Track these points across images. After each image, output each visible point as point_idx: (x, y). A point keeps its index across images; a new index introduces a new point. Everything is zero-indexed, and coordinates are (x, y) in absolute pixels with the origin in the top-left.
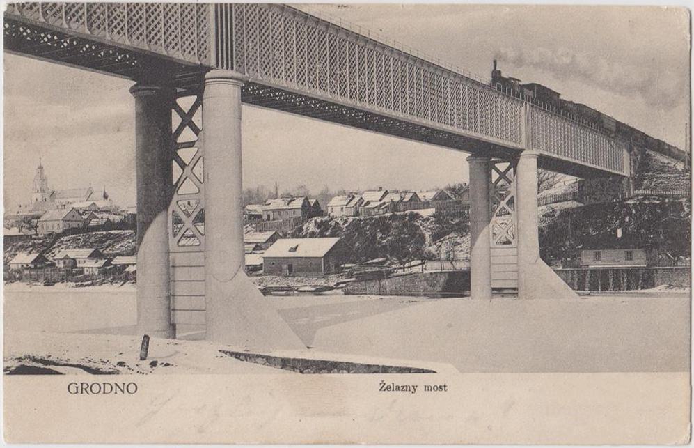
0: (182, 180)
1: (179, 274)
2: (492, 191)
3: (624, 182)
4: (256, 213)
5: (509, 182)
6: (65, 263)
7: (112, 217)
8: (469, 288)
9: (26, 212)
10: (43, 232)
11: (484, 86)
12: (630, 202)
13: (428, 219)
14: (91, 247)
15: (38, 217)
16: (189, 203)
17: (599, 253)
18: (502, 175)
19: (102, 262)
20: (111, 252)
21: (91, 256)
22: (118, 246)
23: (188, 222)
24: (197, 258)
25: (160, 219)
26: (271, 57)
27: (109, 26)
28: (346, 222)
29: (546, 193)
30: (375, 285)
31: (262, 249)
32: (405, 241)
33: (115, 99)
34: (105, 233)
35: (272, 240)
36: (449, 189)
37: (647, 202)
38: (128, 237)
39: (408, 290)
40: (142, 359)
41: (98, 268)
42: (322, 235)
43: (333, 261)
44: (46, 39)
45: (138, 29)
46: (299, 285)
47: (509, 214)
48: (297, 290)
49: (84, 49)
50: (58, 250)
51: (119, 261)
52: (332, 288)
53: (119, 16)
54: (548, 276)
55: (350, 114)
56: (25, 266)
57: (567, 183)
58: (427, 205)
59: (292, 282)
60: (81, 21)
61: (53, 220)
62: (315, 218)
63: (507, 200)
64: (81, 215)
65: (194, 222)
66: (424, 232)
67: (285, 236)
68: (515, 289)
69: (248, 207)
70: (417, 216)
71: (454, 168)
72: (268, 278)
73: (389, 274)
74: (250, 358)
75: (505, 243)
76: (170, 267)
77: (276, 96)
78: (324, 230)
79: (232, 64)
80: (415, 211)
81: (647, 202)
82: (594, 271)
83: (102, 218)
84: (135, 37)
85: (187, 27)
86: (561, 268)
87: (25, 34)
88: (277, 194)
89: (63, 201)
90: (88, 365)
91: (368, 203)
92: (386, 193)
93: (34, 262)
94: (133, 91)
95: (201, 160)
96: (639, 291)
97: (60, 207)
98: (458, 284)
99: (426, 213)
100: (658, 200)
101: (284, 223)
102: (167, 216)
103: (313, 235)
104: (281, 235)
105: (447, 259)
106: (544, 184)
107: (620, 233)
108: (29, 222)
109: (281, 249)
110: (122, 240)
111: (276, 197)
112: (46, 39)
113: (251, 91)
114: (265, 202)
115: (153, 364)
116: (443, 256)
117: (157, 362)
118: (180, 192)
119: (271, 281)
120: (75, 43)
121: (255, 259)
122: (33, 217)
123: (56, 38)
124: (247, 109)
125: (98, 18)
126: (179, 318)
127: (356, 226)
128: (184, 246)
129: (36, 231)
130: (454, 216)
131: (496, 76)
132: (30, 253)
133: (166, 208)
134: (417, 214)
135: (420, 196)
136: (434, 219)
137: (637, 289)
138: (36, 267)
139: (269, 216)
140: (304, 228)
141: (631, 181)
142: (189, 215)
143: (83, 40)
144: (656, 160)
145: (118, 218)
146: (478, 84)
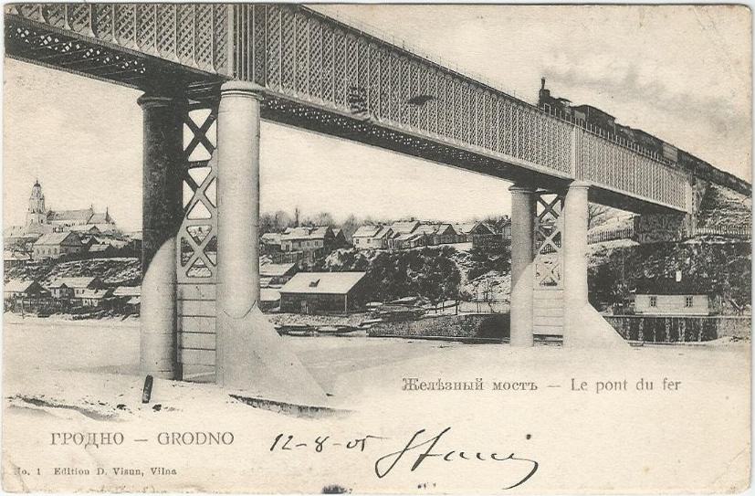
0: (194, 201)
1: (188, 308)
2: (536, 228)
3: (686, 219)
4: (274, 243)
5: (556, 216)
6: (61, 292)
7: (114, 243)
9: (18, 234)
10: (38, 258)
11: (530, 107)
13: (465, 255)
14: (92, 276)
15: (34, 241)
16: (200, 229)
17: (655, 299)
18: (549, 208)
19: (102, 293)
20: (112, 281)
21: (91, 286)
22: (120, 275)
23: (199, 249)
24: (208, 291)
26: (294, 69)
27: (116, 29)
28: (373, 253)
29: (597, 229)
30: (402, 327)
31: (278, 283)
32: (438, 279)
33: (119, 113)
34: (106, 260)
35: (291, 273)
36: (489, 222)
37: (710, 242)
38: (132, 265)
39: (439, 334)
40: (144, 402)
41: (98, 299)
42: (345, 269)
44: (46, 42)
45: (147, 33)
46: (319, 324)
47: (555, 251)
48: (317, 330)
49: (88, 54)
50: (54, 277)
51: (121, 292)
52: (355, 329)
53: (127, 18)
54: (597, 325)
55: (381, 133)
56: (18, 294)
57: (621, 219)
58: (463, 239)
60: (86, 23)
61: (50, 243)
62: (339, 250)
63: (552, 237)
64: (82, 239)
65: (205, 250)
66: (461, 269)
67: (305, 270)
68: (558, 336)
69: (265, 236)
70: (453, 251)
71: (490, 199)
72: (286, 316)
73: (418, 316)
74: (264, 404)
75: (549, 284)
76: (176, 299)
77: (298, 112)
78: (348, 264)
79: (251, 75)
80: (450, 245)
81: (710, 242)
82: (649, 319)
83: (103, 243)
84: (144, 41)
85: (202, 31)
86: (612, 315)
87: (23, 35)
88: (297, 222)
89: (62, 223)
90: (85, 407)
91: (398, 235)
92: (419, 224)
93: (29, 290)
94: (140, 102)
95: (214, 183)
96: (699, 343)
97: (57, 230)
98: (494, 329)
100: (723, 240)
102: (175, 244)
103: (336, 269)
104: (300, 267)
105: (486, 300)
106: (597, 218)
107: (679, 277)
108: (23, 246)
109: (299, 284)
110: (126, 268)
111: (296, 225)
112: (46, 42)
113: (272, 105)
114: (284, 231)
116: (480, 297)
117: (160, 406)
118: (190, 216)
119: (288, 319)
120: (78, 47)
121: (272, 295)
122: (27, 240)
123: (57, 40)
125: (104, 19)
126: (187, 357)
127: (384, 260)
128: (193, 276)
129: (31, 256)
130: (494, 252)
131: (544, 94)
132: (23, 279)
133: (175, 235)
134: (453, 249)
135: (456, 229)
136: (471, 255)
137: (697, 340)
138: (29, 297)
139: (287, 246)
140: (327, 260)
141: (693, 218)
142: (199, 242)
143: (86, 45)
144: (721, 195)
145: (121, 244)
146: (524, 104)
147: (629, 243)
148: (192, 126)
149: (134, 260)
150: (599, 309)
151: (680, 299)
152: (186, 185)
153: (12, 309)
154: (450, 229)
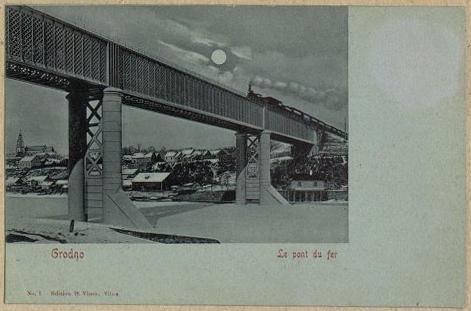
1: (90, 189)
8: (235, 198)
12: (316, 157)
19: (50, 183)
23: (94, 163)
25: (80, 162)
30: (187, 196)
33: (58, 102)
35: (137, 173)
39: (205, 199)
42: (161, 171)
43: (165, 186)
51: (59, 182)
58: (214, 157)
59: (145, 194)
65: (98, 163)
67: (143, 171)
70: (210, 163)
71: (228, 138)
72: (134, 192)
73: (194, 191)
78: (162, 169)
82: (298, 192)
94: (67, 97)
98: (229, 197)
99: (214, 161)
101: (142, 165)
103: (157, 171)
109: (140, 178)
111: (138, 151)
115: (76, 234)
121: (128, 183)
124: (125, 108)
126: (89, 212)
131: (251, 93)
135: (212, 153)
143: (42, 72)
147: (289, 158)
148: (91, 108)
149: (64, 168)
150: (276, 187)
151: (312, 183)
152: (88, 135)
153: (10, 191)
154: (209, 153)
